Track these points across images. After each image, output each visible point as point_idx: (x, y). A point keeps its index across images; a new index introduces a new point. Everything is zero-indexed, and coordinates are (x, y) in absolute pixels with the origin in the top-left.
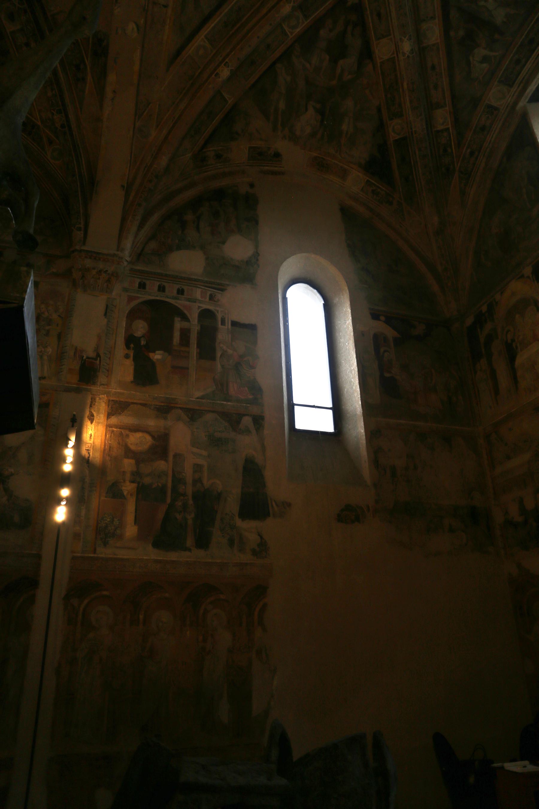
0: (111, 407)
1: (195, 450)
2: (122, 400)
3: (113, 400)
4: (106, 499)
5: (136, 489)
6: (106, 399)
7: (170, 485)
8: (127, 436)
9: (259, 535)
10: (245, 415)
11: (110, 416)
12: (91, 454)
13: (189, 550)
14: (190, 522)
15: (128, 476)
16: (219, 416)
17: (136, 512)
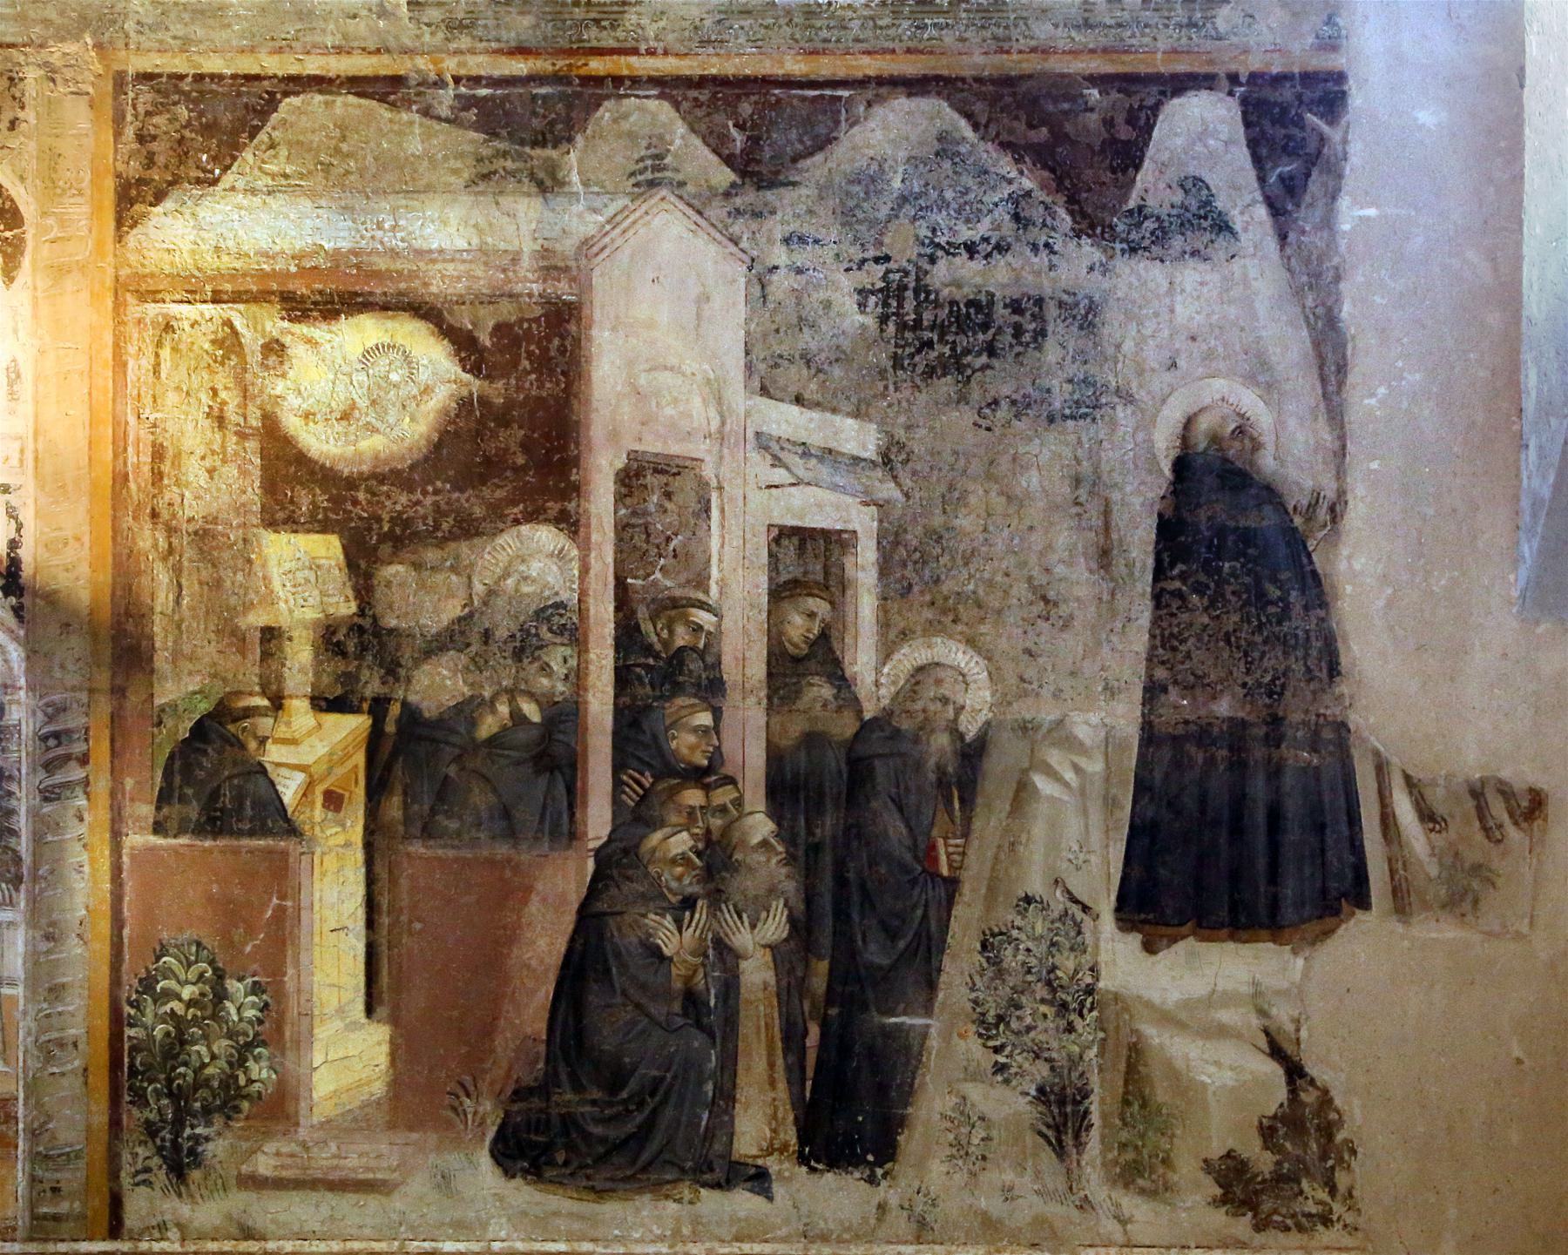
0: (141, 138)
1: (785, 419)
2: (214, 64)
3: (146, 77)
4: (160, 841)
5: (360, 759)
6: (98, 68)
7: (600, 704)
8: (275, 349)
9: (1276, 1051)
10: (1180, 84)
11: (139, 208)
12: (27, 516)
13: (759, 1180)
14: (757, 973)
15: (300, 657)
16: (969, 116)
17: (370, 924)
